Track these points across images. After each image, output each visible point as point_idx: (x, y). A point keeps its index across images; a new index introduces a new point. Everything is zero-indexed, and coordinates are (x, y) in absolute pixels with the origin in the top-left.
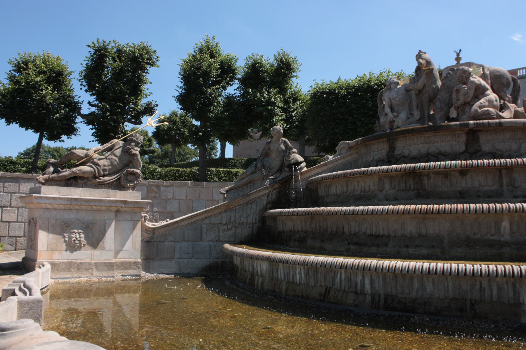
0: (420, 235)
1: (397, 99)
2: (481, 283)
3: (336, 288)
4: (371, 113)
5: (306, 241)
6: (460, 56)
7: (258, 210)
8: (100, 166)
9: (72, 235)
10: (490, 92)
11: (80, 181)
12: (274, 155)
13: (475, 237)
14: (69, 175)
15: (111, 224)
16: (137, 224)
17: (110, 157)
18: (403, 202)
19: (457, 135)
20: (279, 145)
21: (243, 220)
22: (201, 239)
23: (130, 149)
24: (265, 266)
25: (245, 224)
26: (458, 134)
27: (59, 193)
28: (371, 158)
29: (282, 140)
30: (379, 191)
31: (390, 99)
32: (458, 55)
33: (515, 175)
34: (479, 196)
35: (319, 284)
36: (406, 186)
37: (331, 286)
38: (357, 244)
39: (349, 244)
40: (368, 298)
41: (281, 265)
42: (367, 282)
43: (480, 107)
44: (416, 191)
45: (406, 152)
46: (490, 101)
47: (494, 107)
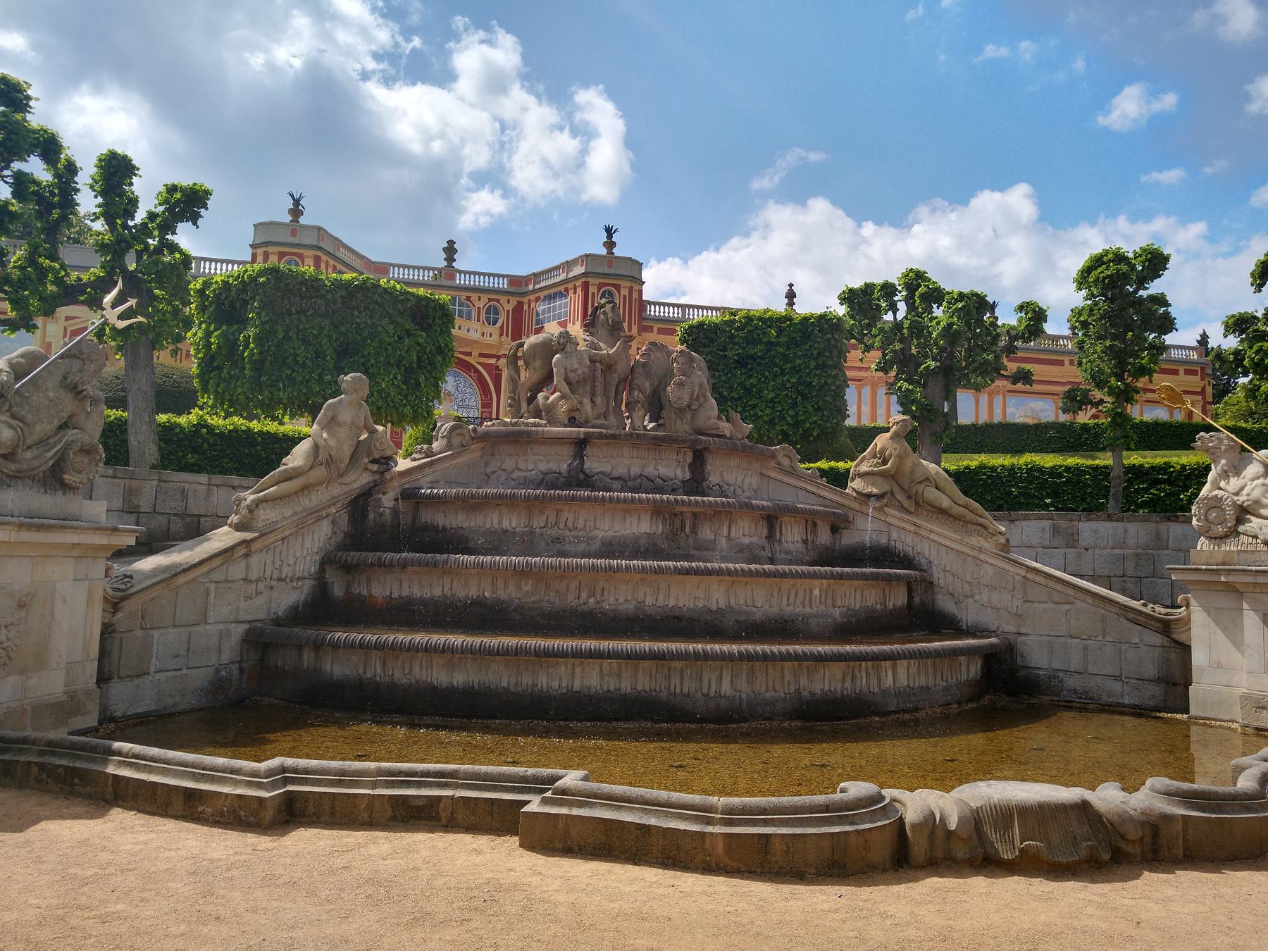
25: (288, 580)
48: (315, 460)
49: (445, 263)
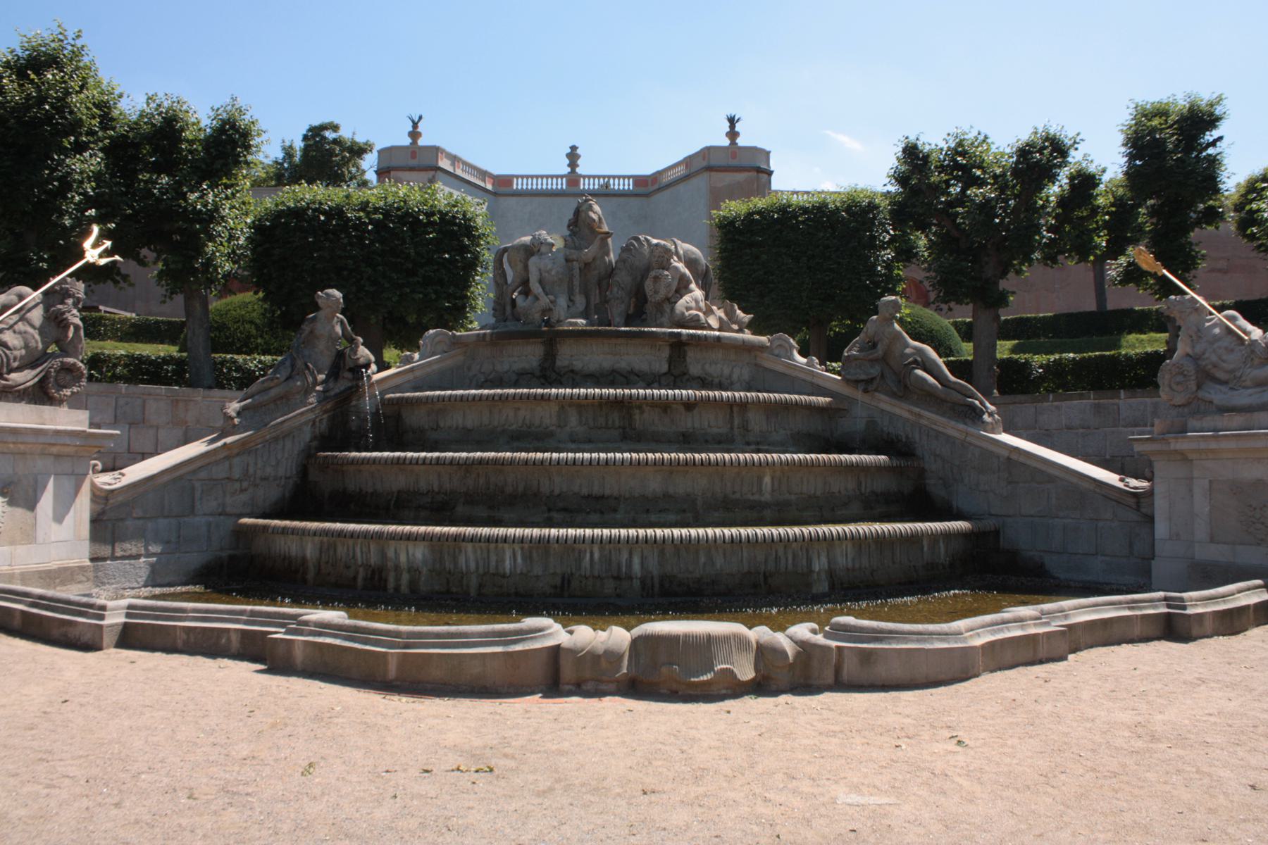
0: (667, 496)
1: (553, 273)
2: (776, 552)
3: (583, 574)
4: (410, 266)
5: (454, 508)
6: (419, 130)
7: (296, 452)
10: (693, 286)
12: (321, 345)
16: (83, 481)
18: (601, 445)
21: (269, 471)
22: (192, 511)
23: (64, 313)
24: (419, 553)
26: (660, 346)
28: (506, 367)
29: (338, 317)
30: (559, 426)
31: (540, 270)
32: (415, 125)
34: (707, 441)
35: (552, 571)
36: (607, 424)
37: (574, 571)
38: (565, 510)
39: (549, 510)
40: (637, 583)
41: (469, 546)
42: (636, 561)
43: (688, 309)
45: (578, 365)
46: (697, 301)
47: (699, 309)
48: (292, 371)
49: (569, 170)
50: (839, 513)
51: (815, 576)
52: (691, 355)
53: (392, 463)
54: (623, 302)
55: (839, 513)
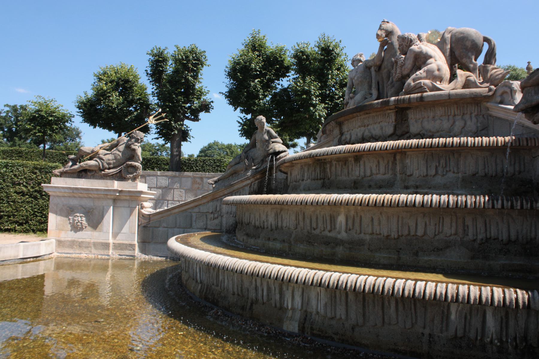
8: (103, 160)
9: (75, 218)
11: (88, 173)
13: (315, 233)
14: (78, 168)
15: (109, 209)
16: (133, 210)
17: (115, 152)
19: (387, 115)
20: (263, 135)
23: (130, 145)
27: (66, 183)
33: (408, 161)
34: (370, 186)
44: (322, 180)
50: (426, 258)
51: (290, 313)
52: (411, 115)
53: (264, 204)
54: (393, 86)
55: (426, 258)
